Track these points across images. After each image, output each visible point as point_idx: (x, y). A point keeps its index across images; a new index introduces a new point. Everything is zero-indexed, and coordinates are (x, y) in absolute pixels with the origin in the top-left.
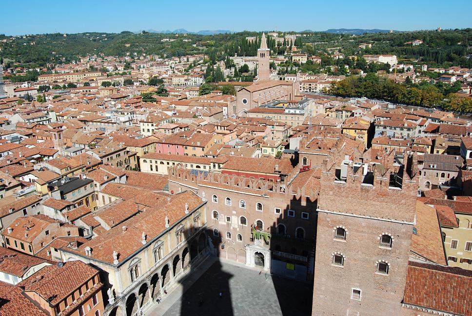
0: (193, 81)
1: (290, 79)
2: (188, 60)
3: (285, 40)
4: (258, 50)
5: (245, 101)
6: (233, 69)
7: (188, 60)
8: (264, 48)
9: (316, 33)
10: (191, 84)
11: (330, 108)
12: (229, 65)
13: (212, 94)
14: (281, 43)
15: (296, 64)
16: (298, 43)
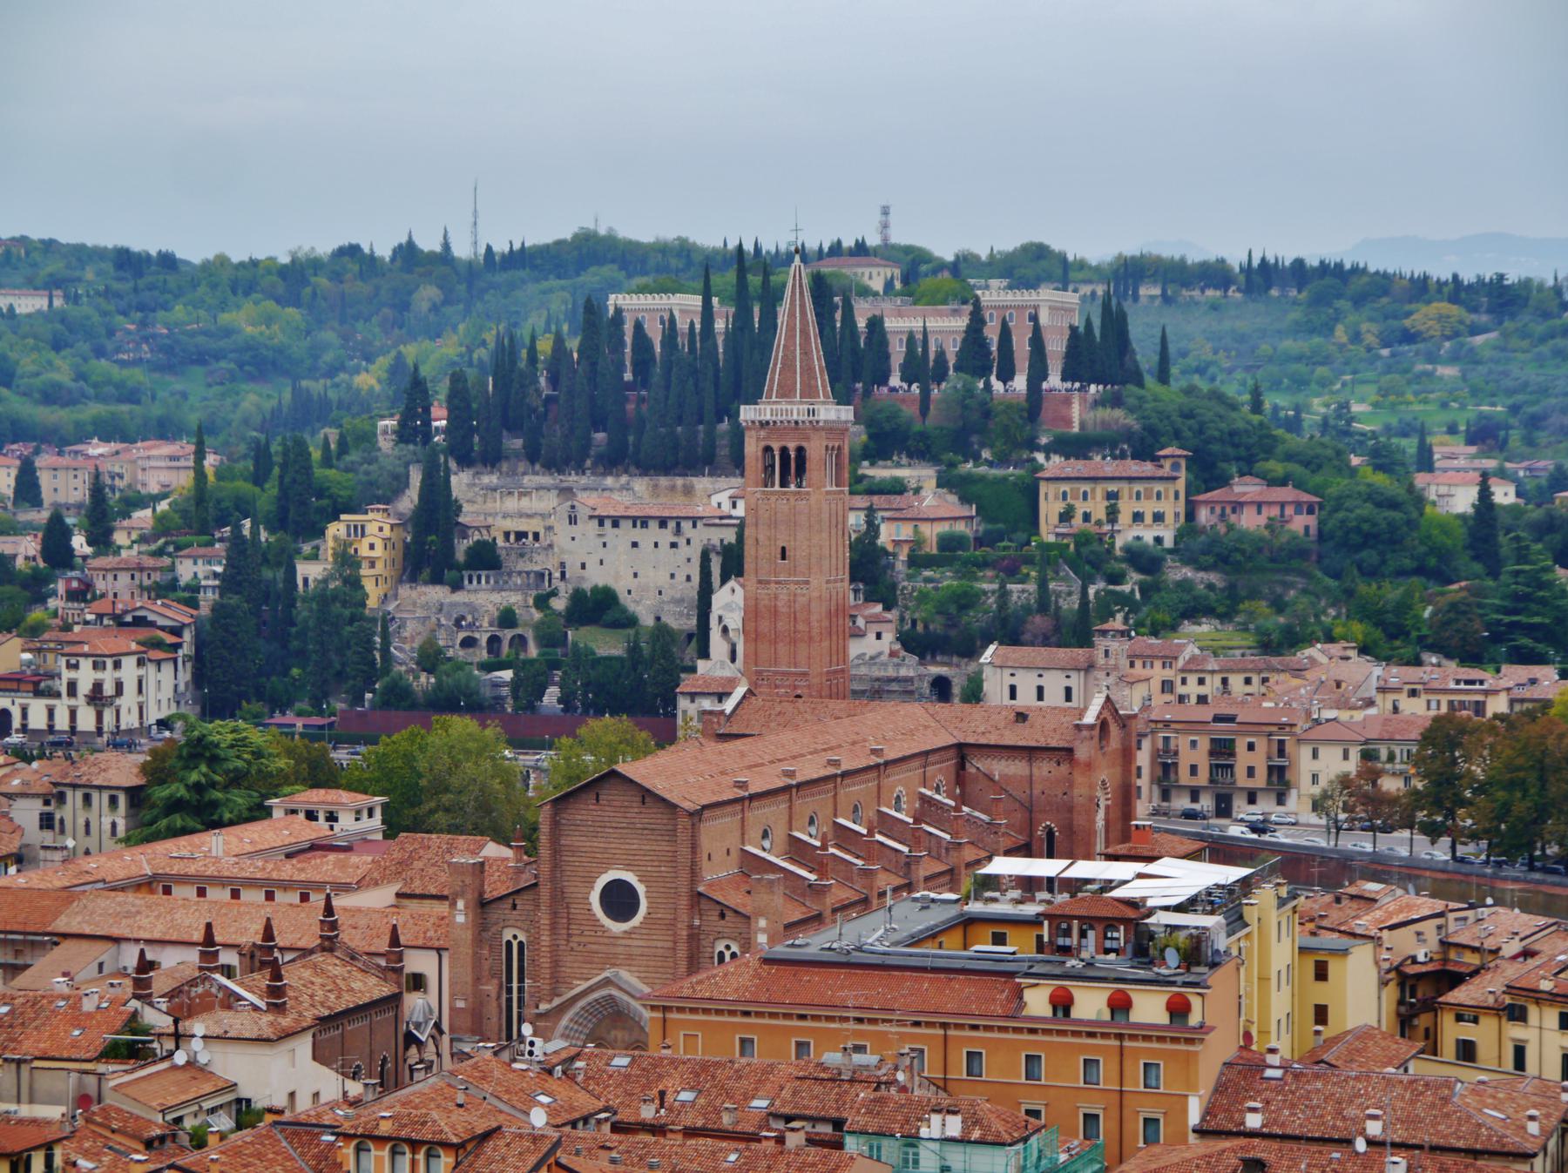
0: (84, 688)
1: (1054, 697)
2: (27, 489)
3: (977, 320)
4: (747, 413)
5: (620, 900)
6: (485, 598)
7: (27, 489)
8: (797, 404)
9: (1262, 277)
10: (62, 723)
11: (1456, 979)
12: (435, 549)
13: (281, 828)
14: (941, 355)
15: (1090, 555)
16: (1100, 354)
